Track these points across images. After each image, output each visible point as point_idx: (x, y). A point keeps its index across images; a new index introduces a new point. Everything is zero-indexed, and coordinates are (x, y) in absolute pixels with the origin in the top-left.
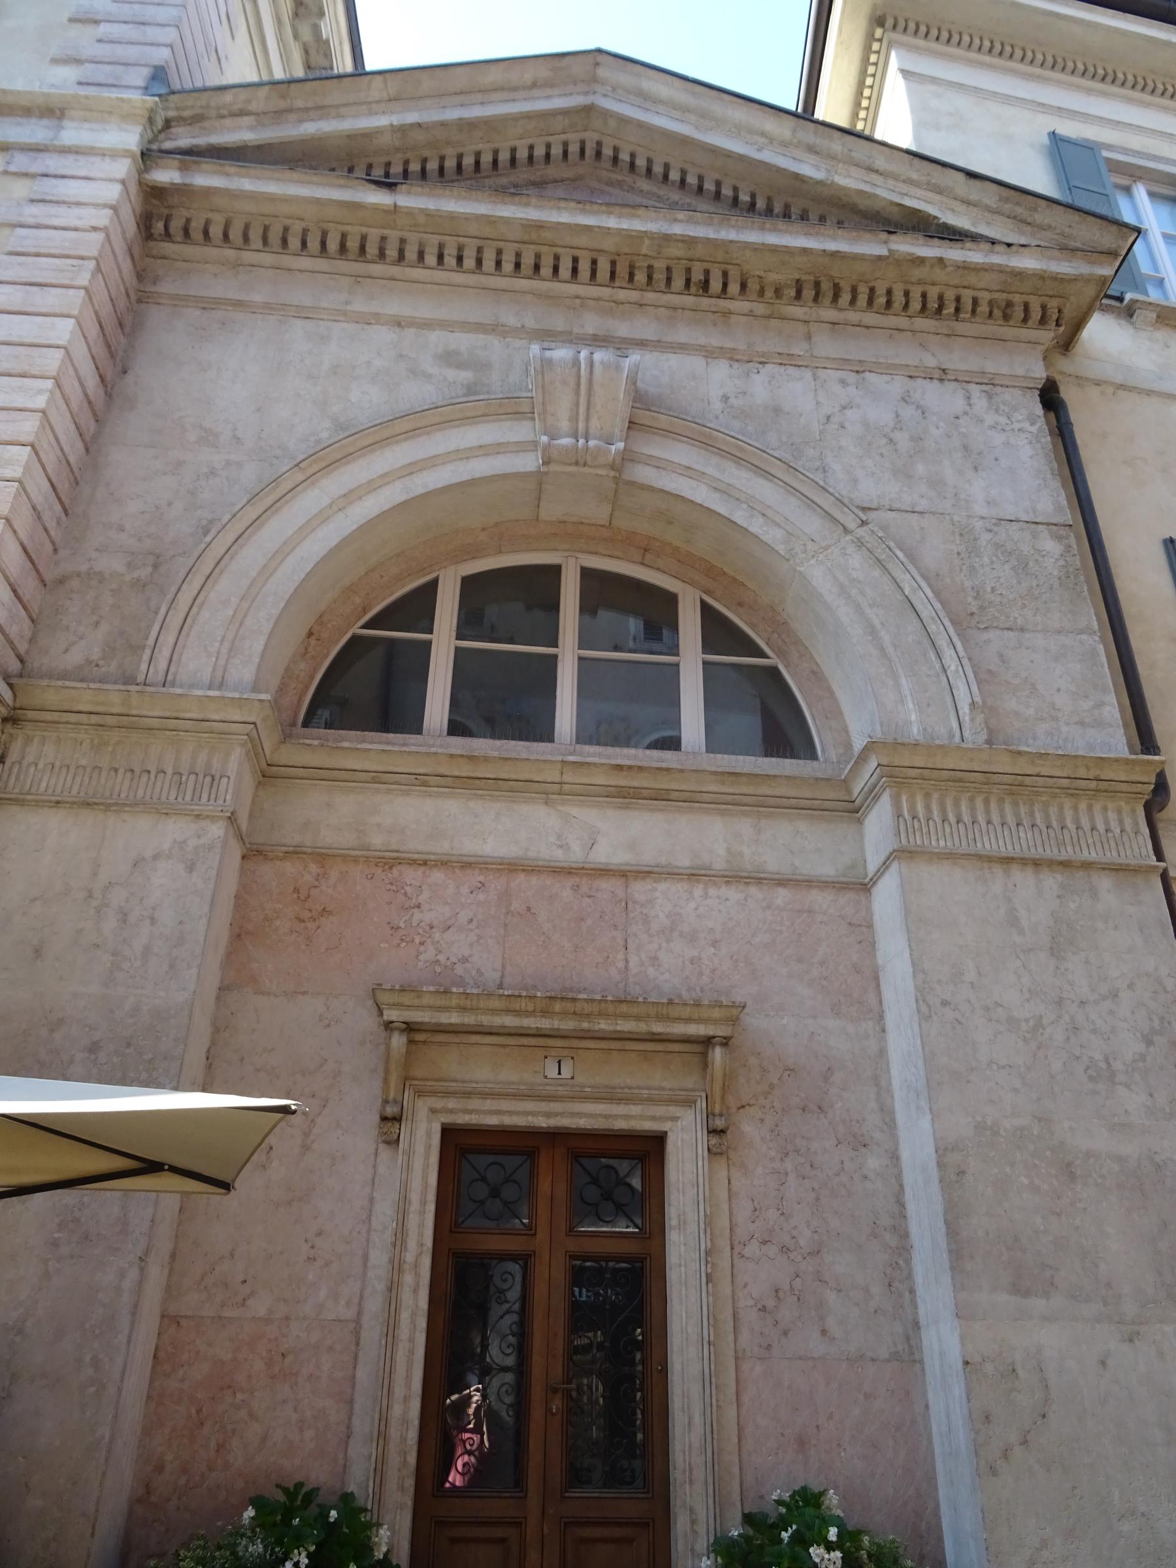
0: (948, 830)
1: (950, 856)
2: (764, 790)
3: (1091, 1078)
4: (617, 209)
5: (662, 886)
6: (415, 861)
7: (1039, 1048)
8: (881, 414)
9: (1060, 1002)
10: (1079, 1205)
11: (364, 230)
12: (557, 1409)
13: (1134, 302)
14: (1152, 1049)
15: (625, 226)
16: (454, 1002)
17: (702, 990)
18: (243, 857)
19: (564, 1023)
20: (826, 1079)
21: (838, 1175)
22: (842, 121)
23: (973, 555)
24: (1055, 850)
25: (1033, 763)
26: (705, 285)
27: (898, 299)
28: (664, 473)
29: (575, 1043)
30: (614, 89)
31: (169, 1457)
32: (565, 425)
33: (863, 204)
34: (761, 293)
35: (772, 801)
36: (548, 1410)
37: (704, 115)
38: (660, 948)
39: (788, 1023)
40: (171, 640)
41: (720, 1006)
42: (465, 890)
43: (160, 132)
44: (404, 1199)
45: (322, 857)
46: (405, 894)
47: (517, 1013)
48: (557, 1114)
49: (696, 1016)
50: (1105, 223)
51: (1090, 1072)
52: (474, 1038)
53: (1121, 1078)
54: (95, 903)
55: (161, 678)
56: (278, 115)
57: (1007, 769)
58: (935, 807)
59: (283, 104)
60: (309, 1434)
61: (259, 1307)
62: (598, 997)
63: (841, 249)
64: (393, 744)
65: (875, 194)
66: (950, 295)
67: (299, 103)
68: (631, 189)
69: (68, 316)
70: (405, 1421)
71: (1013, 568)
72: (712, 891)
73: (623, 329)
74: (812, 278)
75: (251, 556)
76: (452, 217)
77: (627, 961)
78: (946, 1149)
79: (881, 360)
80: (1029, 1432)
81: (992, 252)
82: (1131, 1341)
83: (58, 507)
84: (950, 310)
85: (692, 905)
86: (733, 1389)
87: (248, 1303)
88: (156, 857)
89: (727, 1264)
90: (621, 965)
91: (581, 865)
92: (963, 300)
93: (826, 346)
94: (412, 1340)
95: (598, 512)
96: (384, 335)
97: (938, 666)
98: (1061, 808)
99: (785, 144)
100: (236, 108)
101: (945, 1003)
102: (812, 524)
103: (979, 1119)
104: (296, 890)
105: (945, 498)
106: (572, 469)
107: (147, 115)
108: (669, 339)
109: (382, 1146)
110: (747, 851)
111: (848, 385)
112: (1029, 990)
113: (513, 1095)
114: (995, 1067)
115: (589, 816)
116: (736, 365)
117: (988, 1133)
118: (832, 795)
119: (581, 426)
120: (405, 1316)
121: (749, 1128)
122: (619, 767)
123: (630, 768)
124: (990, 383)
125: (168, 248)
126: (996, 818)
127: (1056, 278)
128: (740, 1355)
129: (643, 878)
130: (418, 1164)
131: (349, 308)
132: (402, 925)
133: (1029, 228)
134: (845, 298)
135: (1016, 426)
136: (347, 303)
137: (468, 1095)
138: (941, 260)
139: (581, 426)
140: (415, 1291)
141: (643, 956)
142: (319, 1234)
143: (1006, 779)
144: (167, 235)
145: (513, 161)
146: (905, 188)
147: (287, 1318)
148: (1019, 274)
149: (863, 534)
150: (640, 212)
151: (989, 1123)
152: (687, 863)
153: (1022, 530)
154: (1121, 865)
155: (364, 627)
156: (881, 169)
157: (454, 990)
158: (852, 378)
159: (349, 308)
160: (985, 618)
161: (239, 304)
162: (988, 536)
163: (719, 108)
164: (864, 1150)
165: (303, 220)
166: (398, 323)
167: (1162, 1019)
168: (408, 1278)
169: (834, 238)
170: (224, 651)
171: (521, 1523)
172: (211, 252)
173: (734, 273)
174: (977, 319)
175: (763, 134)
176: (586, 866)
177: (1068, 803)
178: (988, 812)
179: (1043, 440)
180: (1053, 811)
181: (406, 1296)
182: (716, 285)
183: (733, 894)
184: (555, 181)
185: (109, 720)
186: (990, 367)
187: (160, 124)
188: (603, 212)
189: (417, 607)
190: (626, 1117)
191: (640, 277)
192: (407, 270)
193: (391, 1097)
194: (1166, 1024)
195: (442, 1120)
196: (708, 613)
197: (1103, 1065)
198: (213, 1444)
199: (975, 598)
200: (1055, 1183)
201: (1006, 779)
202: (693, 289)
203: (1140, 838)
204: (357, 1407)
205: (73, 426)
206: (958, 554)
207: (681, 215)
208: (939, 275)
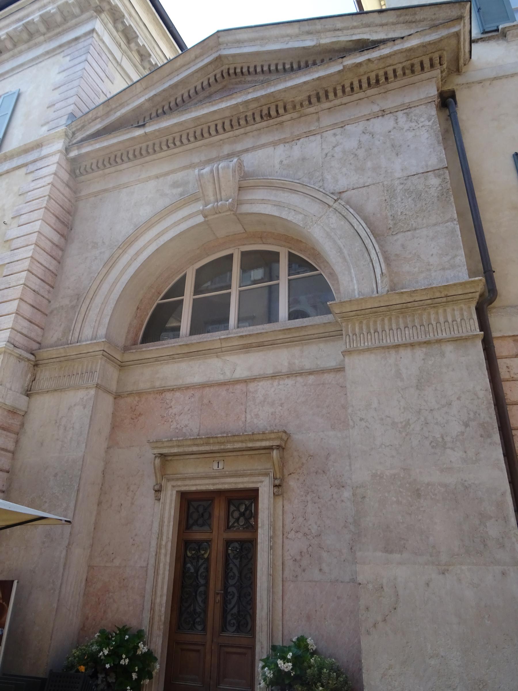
0: (369, 337)
1: (369, 350)
2: (303, 333)
3: (433, 447)
4: (225, 98)
5: (261, 384)
6: (169, 389)
7: (406, 435)
8: (351, 144)
9: (419, 412)
10: (421, 509)
11: (140, 145)
12: (219, 601)
13: (504, 29)
14: (468, 429)
15: (228, 105)
16: (175, 444)
17: (276, 426)
18: (115, 398)
19: (217, 447)
20: (327, 458)
21: (330, 501)
22: (139, 78)
23: (392, 199)
24: (423, 336)
25: (411, 296)
26: (269, 115)
27: (356, 85)
28: (253, 205)
29: (224, 454)
30: (227, 45)
31: (90, 615)
32: (212, 198)
33: (337, 47)
34: (294, 107)
35: (307, 337)
36: (215, 601)
37: (262, 39)
38: (259, 410)
39: (311, 435)
40: (80, 326)
41: (273, 433)
42: (187, 398)
43: (72, 138)
44: (162, 521)
45: (139, 394)
46: (167, 403)
47: (197, 445)
48: (217, 484)
49: (265, 438)
50: (452, 5)
51: (433, 444)
52: (188, 457)
53: (449, 445)
54: (57, 424)
55: (76, 340)
56: (107, 114)
57: (398, 302)
58: (364, 327)
59: (108, 109)
60: (131, 608)
61: (117, 562)
62: (251, 433)
63: (320, 75)
64: (164, 345)
65: (339, 41)
66: (381, 73)
67: (114, 106)
68: (245, 82)
69: (39, 220)
70: (161, 604)
71: (413, 200)
72: (281, 382)
73: (239, 147)
74: (315, 92)
75: (106, 287)
76: (166, 128)
77: (246, 417)
78: (357, 487)
79: (352, 118)
80: (387, 616)
81: (395, 45)
82: (443, 573)
83: (47, 287)
84: (382, 80)
85: (273, 389)
86: (281, 594)
87: (114, 560)
88: (75, 405)
89: (280, 541)
90: (243, 419)
91: (228, 380)
92: (388, 73)
93: (326, 120)
94: (164, 574)
95: (239, 229)
96: (152, 184)
97: (368, 259)
98: (429, 314)
99: (297, 36)
100: (93, 118)
101: (361, 419)
102: (314, 208)
103: (374, 472)
104: (131, 408)
105: (380, 174)
106: (216, 216)
107: (64, 134)
108: (258, 144)
109: (156, 501)
110: (297, 362)
111: (337, 135)
112: (404, 408)
113: (203, 477)
114: (383, 446)
115: (232, 359)
116: (287, 145)
117: (378, 478)
118: (333, 329)
119: (218, 197)
120: (161, 565)
121: (292, 483)
122: (242, 337)
123: (246, 336)
124: (407, 108)
125: (82, 178)
126: (394, 326)
127: (430, 43)
128: (285, 579)
129: (253, 381)
130: (167, 508)
131: (140, 178)
132: (165, 415)
133: (414, 24)
134: (331, 95)
135: (421, 125)
136: (139, 176)
137: (184, 479)
138: (369, 60)
139: (218, 197)
140: (166, 555)
141: (253, 415)
142: (136, 535)
143: (398, 307)
144: (81, 174)
145: (196, 92)
146: (352, 32)
147: (125, 566)
148: (411, 50)
149: (336, 206)
150: (234, 96)
151: (379, 473)
152: (271, 372)
153: (419, 178)
154: (457, 337)
155: (161, 300)
156: (340, 28)
157: (174, 439)
158: (338, 131)
159: (140, 178)
160: (396, 229)
161: (105, 191)
162: (401, 187)
163: (267, 33)
164: (343, 489)
165: (120, 150)
166: (157, 177)
167: (475, 413)
168: (163, 551)
169: (317, 71)
170: (97, 325)
171: (204, 645)
172: (95, 174)
173: (281, 104)
174: (398, 79)
175: (288, 36)
176: (231, 380)
177: (432, 311)
178: (390, 324)
179: (435, 127)
180: (425, 317)
181: (162, 557)
182: (273, 113)
183: (290, 382)
184: (215, 92)
185: (62, 359)
186: (407, 100)
187: (70, 135)
188: (220, 102)
189: (178, 288)
190: (243, 483)
191: (242, 122)
192: (158, 154)
193: (159, 482)
194: (477, 415)
195: (177, 490)
196: (292, 258)
197: (440, 440)
198: (103, 610)
199: (392, 220)
200: (410, 499)
201: (398, 307)
202: (265, 118)
203: (472, 321)
204: (146, 598)
205: (49, 256)
206: (385, 200)
207: (250, 90)
208: (372, 66)
